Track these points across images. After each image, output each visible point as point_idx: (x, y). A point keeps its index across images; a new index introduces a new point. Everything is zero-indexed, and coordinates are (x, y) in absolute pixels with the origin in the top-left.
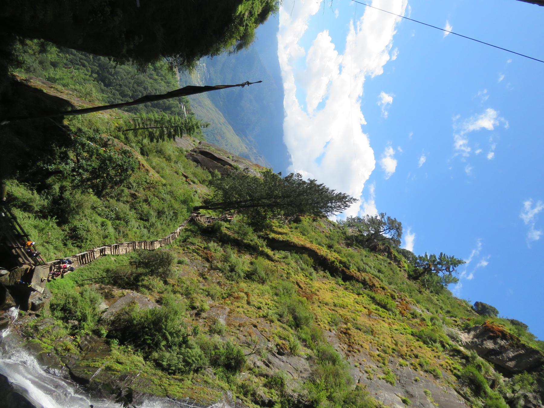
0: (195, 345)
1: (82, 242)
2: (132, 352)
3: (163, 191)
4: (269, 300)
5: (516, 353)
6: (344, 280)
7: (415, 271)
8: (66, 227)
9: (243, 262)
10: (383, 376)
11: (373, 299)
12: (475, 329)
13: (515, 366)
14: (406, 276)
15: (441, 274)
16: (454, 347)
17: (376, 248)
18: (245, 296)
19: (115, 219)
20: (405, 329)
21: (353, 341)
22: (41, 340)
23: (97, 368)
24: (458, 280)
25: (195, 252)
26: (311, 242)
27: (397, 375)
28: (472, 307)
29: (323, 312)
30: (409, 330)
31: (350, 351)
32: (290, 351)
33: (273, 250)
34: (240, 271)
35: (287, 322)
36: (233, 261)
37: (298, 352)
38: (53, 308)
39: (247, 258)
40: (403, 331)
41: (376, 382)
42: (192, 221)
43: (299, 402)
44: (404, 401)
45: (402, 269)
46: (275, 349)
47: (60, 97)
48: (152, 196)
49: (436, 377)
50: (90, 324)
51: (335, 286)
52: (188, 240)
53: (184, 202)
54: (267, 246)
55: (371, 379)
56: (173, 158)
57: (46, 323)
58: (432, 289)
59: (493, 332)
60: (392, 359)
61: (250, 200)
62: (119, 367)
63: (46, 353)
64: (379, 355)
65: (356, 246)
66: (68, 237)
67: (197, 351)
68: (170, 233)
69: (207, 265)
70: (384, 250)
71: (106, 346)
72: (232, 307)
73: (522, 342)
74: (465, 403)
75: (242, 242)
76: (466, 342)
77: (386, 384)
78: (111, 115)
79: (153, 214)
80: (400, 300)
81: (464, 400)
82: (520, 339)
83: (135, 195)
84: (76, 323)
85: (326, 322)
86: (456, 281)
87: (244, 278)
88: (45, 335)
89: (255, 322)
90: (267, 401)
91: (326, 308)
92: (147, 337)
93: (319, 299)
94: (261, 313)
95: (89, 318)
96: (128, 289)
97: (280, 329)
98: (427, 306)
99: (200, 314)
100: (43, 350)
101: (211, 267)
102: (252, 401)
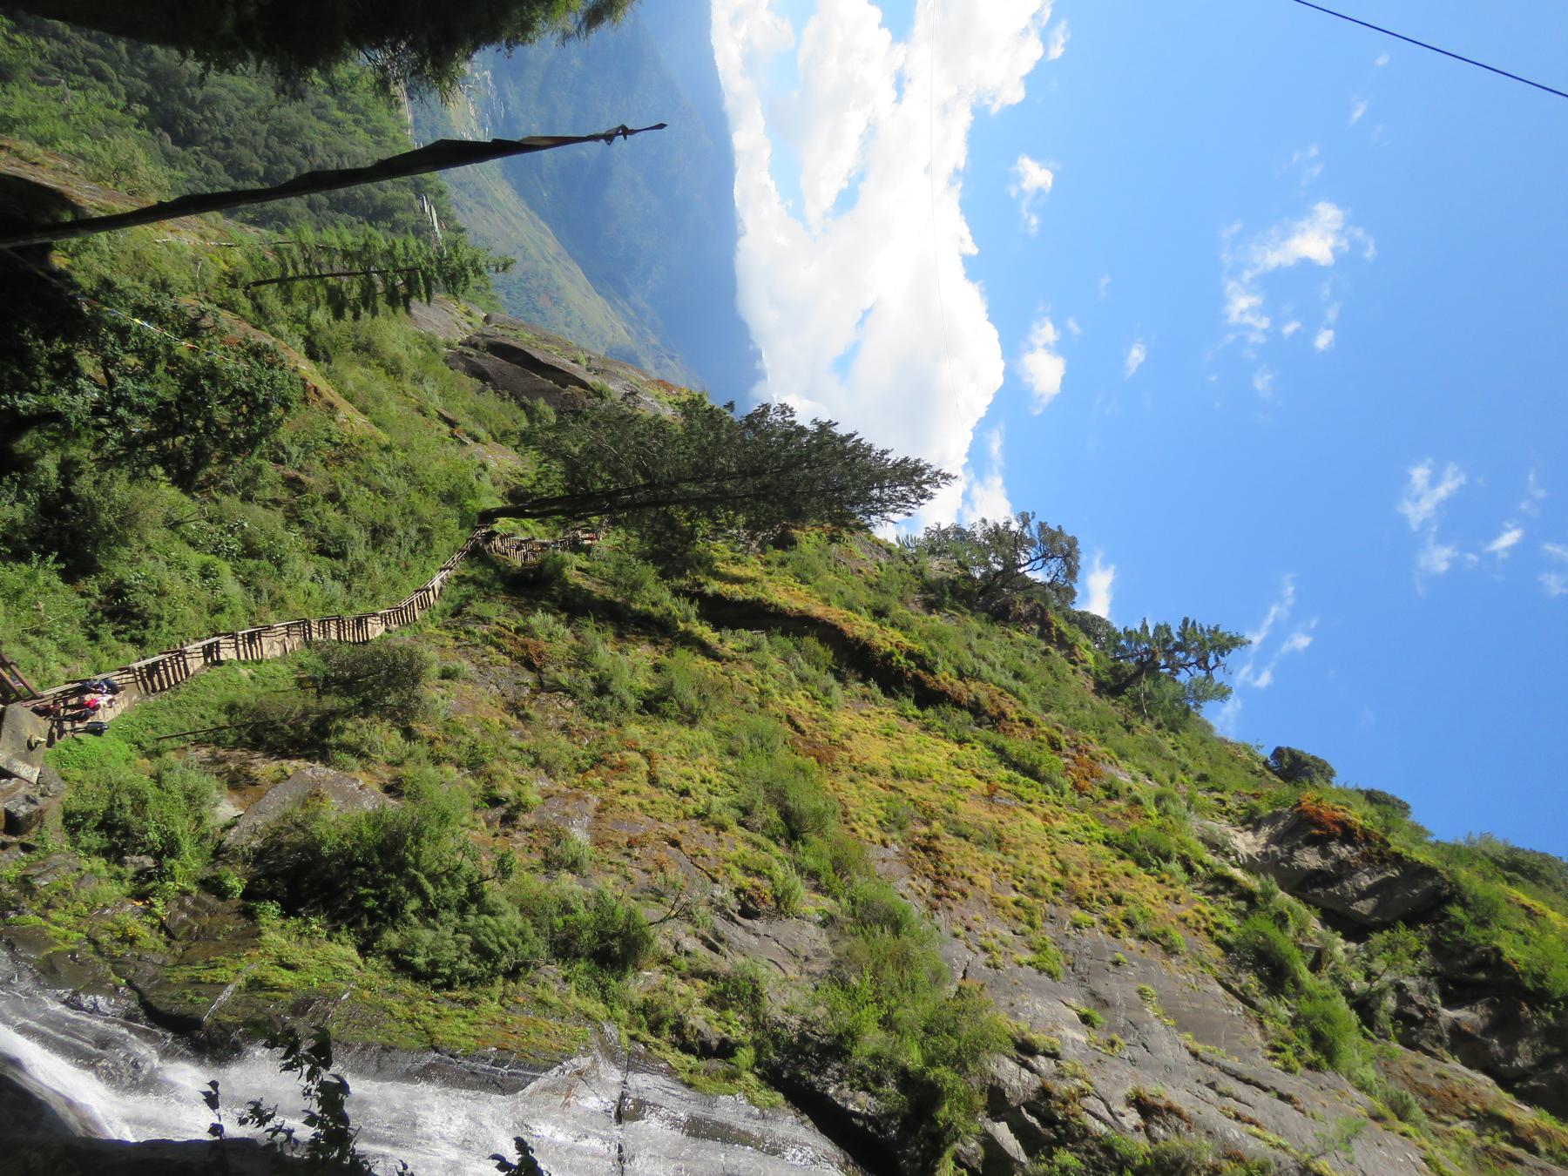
0: (506, 905)
1: (146, 625)
2: (323, 933)
3: (384, 466)
4: (711, 769)
5: (1378, 878)
6: (922, 703)
7: (1114, 671)
8: (92, 585)
9: (632, 665)
10: (1029, 956)
11: (1000, 751)
12: (1273, 819)
13: (1375, 911)
14: (1091, 685)
15: (1183, 677)
16: (1217, 871)
17: (1009, 612)
18: (643, 762)
20: (1086, 829)
21: (948, 868)
22: (45, 917)
23: (221, 984)
24: (1230, 690)
25: (492, 643)
26: (826, 601)
27: (1067, 952)
28: (1265, 763)
29: (862, 796)
30: (1099, 832)
31: (938, 897)
32: (774, 904)
33: (717, 628)
34: (625, 692)
35: (764, 826)
36: (604, 665)
37: (796, 905)
38: (73, 823)
39: (643, 654)
40: (1082, 835)
41: (1011, 972)
42: (476, 554)
43: (804, 1038)
44: (1086, 1020)
45: (1079, 668)
46: (733, 903)
47: (32, 178)
48: (350, 484)
49: (1170, 951)
50: (190, 865)
51: (895, 722)
52: (468, 609)
53: (450, 498)
54: (700, 617)
55: (996, 967)
56: (409, 367)
57: (55, 867)
58: (1160, 718)
59: (1319, 825)
60: (1053, 910)
61: (644, 486)
62: (287, 978)
63: (64, 953)
64: (1016, 903)
66: (99, 614)
67: (512, 918)
68: (411, 589)
69: (529, 678)
70: (1031, 617)
71: (243, 923)
72: (606, 795)
73: (1394, 848)
74: (1245, 1012)
75: (629, 609)
76: (1249, 856)
77: (1038, 977)
78: (202, 237)
79: (358, 535)
80: (1073, 753)
81: (1241, 1006)
82: (1388, 839)
83: (301, 482)
84: (149, 862)
85: (873, 820)
86: (1223, 693)
87: (638, 711)
88: (55, 901)
89: (673, 831)
90: (715, 1043)
91: (871, 784)
92: (363, 891)
94: (691, 806)
95: (187, 846)
96: (298, 757)
97: (743, 848)
98: (1147, 763)
99: (515, 818)
100: (52, 944)
101: (541, 684)
102: (674, 1045)
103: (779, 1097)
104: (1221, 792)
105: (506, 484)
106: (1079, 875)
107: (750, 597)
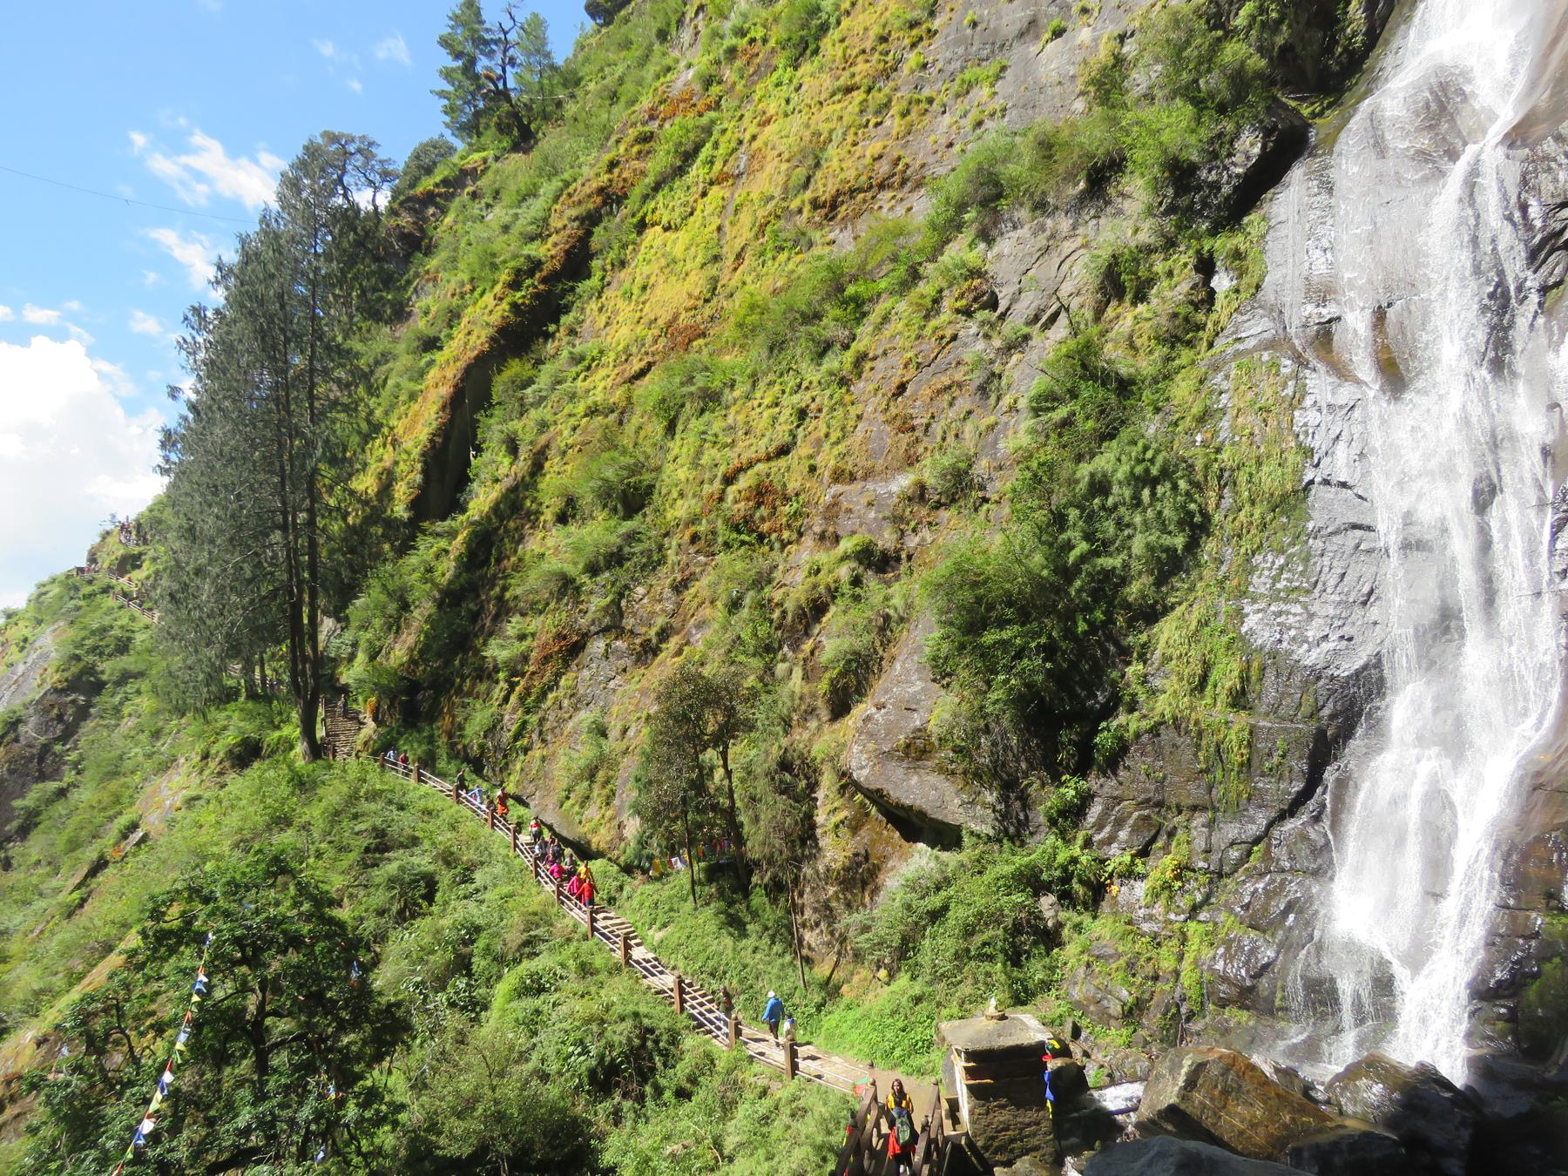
7: (502, 129)
9: (550, 549)
17: (410, 235)
19: (470, 975)
20: (777, 85)
21: (864, 178)
23: (1251, 733)
24: (536, 16)
31: (903, 183)
33: (456, 506)
55: (1005, 109)
65: (405, 288)
68: (457, 807)
69: (597, 646)
89: (879, 401)
92: (1082, 627)
93: (687, 310)
97: (895, 326)
99: (884, 554)
102: (1209, 311)
103: (1252, 218)
104: (683, 14)
105: (220, 774)
106: (853, 75)
107: (419, 466)
